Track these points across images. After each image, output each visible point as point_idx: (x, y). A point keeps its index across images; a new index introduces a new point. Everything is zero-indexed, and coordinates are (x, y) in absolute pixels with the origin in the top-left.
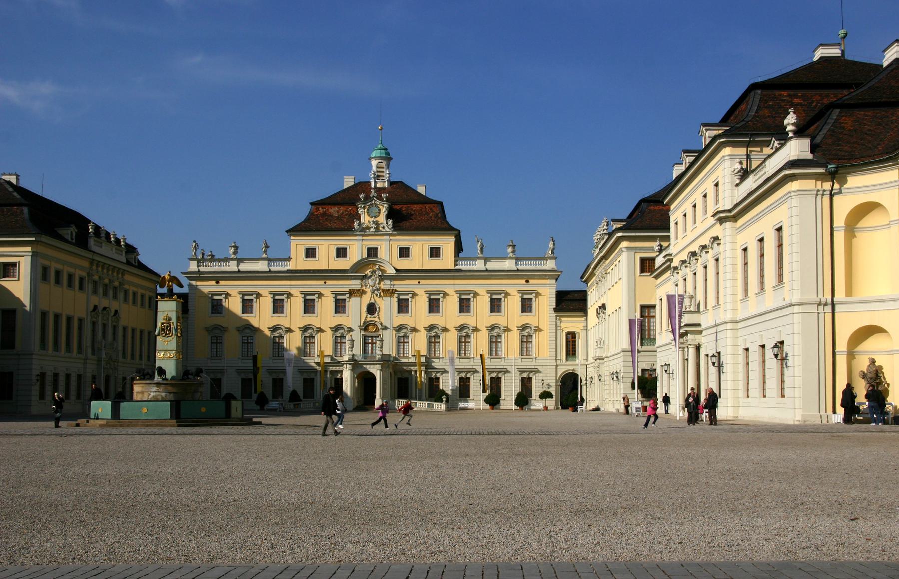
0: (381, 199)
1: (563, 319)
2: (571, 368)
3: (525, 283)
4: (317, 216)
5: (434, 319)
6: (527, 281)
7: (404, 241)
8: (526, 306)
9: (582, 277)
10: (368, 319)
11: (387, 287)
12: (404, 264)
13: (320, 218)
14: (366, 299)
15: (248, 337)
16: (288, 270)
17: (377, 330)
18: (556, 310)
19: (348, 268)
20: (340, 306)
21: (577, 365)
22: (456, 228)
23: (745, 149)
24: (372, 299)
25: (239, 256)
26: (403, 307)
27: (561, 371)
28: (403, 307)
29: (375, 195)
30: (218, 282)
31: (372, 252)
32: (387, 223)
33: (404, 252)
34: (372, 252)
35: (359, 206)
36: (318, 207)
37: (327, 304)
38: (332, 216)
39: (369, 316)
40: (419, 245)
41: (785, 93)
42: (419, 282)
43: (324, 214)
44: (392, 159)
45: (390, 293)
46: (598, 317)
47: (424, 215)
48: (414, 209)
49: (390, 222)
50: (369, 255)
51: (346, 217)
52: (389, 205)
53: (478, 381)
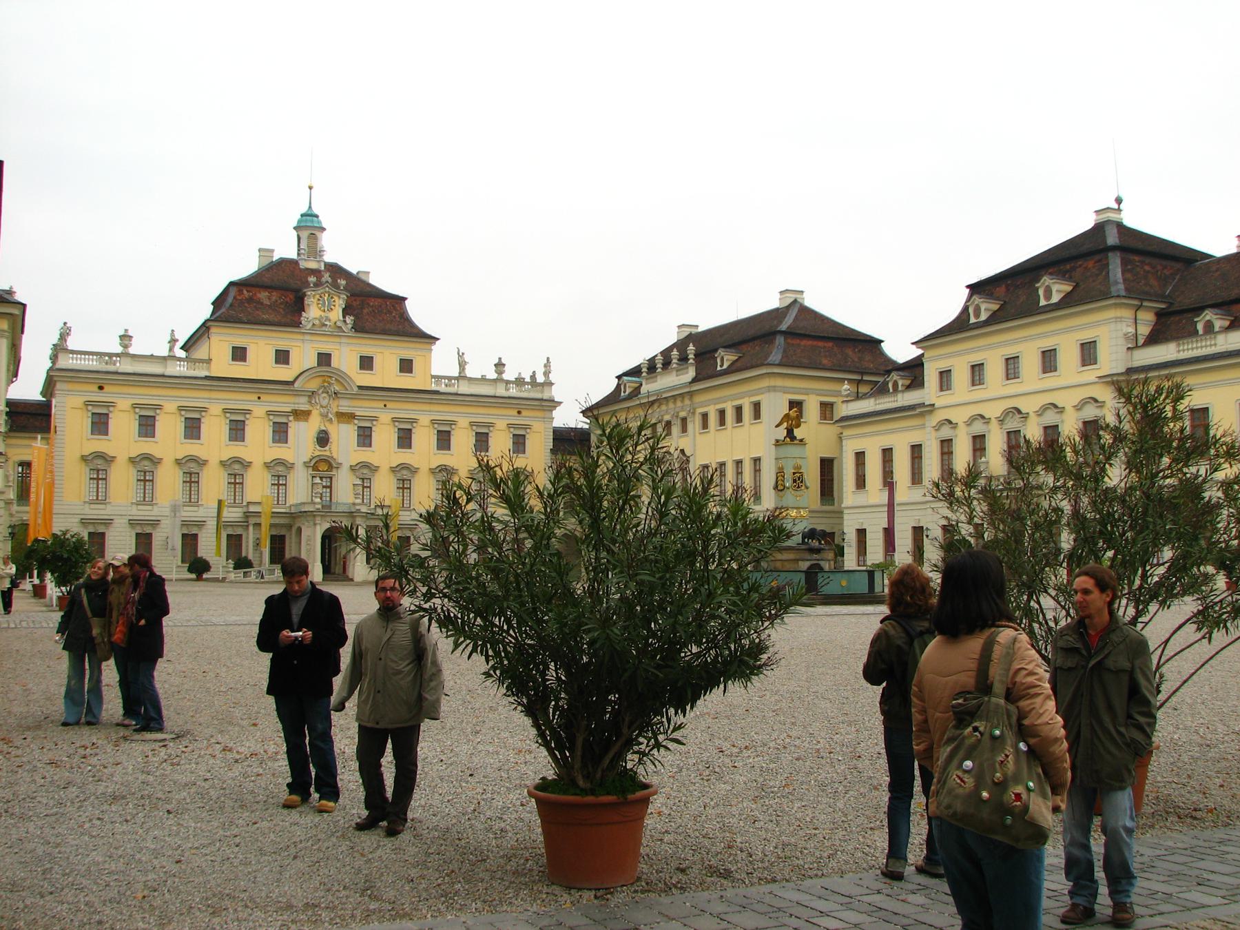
0: (335, 285)
3: (516, 414)
4: (242, 302)
5: (404, 457)
6: (519, 412)
8: (519, 443)
10: (317, 453)
11: (344, 410)
12: (366, 379)
13: (246, 305)
14: (314, 424)
15: (145, 473)
16: (207, 378)
17: (331, 467)
19: (292, 380)
20: (280, 433)
22: (433, 335)
23: (1133, 312)
24: (322, 425)
25: (132, 351)
26: (365, 437)
28: (365, 437)
29: (330, 280)
30: (101, 388)
31: (324, 359)
32: (345, 321)
33: (366, 363)
34: (324, 359)
35: (309, 293)
36: (241, 288)
37: (259, 431)
38: (262, 304)
39: (318, 448)
40: (387, 355)
41: (1137, 258)
42: (385, 406)
43: (250, 300)
44: (324, 229)
45: (351, 417)
48: (371, 304)
49: (349, 319)
50: (319, 364)
51: (282, 306)
52: (347, 296)
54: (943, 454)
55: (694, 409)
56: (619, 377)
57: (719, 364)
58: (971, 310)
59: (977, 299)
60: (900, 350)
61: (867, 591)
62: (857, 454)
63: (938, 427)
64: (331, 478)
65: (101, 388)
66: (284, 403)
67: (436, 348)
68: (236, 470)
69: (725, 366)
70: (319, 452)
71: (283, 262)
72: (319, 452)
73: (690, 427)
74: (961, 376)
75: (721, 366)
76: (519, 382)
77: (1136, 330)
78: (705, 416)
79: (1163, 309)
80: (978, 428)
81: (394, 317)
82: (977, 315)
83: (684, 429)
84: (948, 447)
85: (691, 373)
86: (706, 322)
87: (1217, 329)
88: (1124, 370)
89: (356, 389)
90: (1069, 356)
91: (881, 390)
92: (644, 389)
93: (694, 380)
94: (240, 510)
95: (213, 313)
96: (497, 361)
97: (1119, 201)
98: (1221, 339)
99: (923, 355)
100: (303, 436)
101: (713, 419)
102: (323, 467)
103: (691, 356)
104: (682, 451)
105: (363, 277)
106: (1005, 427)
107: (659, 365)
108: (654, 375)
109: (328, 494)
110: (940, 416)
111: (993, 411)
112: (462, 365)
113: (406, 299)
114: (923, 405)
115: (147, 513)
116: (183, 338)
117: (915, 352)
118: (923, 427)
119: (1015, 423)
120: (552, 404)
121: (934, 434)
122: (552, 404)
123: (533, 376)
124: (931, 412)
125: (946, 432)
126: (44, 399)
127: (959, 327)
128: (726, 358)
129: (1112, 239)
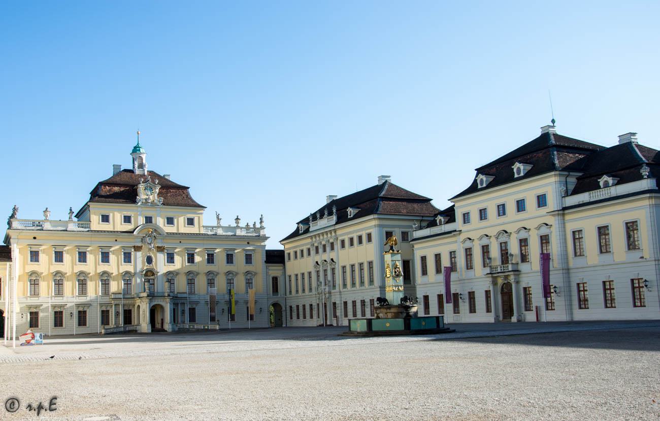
1: (270, 268)
2: (276, 300)
6: (248, 243)
7: (170, 211)
9: (280, 242)
16: (88, 231)
17: (153, 274)
18: (267, 262)
19: (132, 231)
20: (128, 258)
21: (278, 299)
26: (171, 259)
27: (272, 301)
28: (171, 259)
31: (149, 220)
43: (110, 190)
46: (315, 267)
47: (179, 196)
53: (221, 310)
54: (467, 255)
55: (337, 238)
56: (298, 223)
57: (349, 215)
58: (478, 182)
59: (481, 176)
60: (441, 203)
61: (436, 327)
62: (422, 257)
63: (464, 241)
64: (154, 280)
65: (35, 238)
66: (130, 242)
67: (205, 212)
68: (105, 279)
69: (352, 216)
70: (147, 266)
71: (125, 171)
72: (147, 266)
73: (335, 247)
74: (475, 216)
75: (350, 216)
76: (247, 227)
77: (567, 187)
78: (343, 242)
79: (581, 176)
80: (485, 241)
81: (184, 197)
82: (482, 184)
83: (332, 248)
84: (470, 251)
85: (334, 218)
86: (341, 194)
87: (610, 185)
88: (561, 209)
89: (166, 234)
90: (531, 203)
91: (433, 224)
92: (310, 230)
93: (337, 223)
94: (108, 298)
95: (91, 198)
96: (236, 217)
97: (553, 121)
98: (613, 189)
99: (454, 206)
100: (139, 258)
101: (347, 243)
102: (150, 274)
103: (334, 211)
104: (332, 260)
105: (166, 177)
106: (499, 240)
107: (318, 216)
108: (316, 221)
109: (153, 288)
110: (463, 236)
111: (493, 232)
112: (218, 219)
113: (189, 188)
114: (455, 231)
115: (61, 301)
116: (76, 211)
117: (450, 204)
118: (456, 242)
119: (504, 238)
120: (265, 238)
121: (462, 245)
122: (265, 238)
123: (254, 224)
124: (460, 234)
125: (468, 244)
126: (5, 245)
127: (473, 189)
128: (351, 211)
129: (553, 141)
